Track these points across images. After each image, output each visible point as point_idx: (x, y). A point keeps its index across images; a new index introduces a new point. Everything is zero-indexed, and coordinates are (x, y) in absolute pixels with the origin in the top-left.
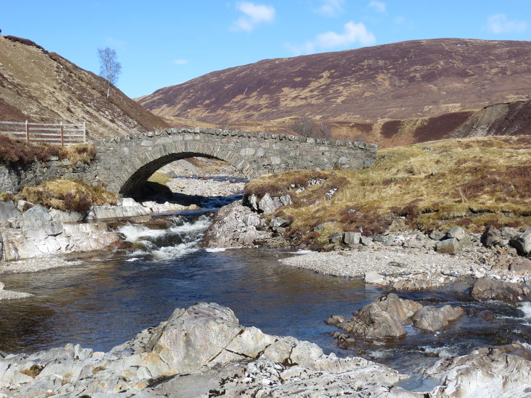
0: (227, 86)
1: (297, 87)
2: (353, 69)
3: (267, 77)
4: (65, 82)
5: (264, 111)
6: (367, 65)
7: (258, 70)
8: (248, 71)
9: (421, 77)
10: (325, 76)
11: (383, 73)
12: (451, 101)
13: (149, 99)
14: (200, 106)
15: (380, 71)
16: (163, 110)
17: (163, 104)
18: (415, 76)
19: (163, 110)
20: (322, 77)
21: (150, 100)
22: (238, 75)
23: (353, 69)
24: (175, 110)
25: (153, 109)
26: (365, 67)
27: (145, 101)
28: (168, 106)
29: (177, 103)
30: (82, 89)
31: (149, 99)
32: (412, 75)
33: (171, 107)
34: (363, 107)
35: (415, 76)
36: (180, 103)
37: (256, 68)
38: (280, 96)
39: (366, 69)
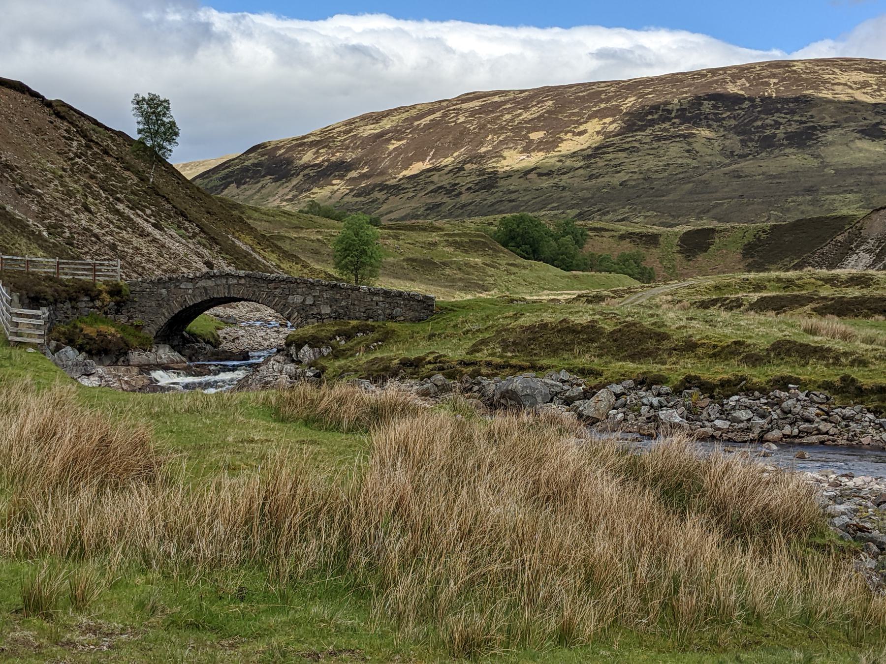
0: (393, 144)
1: (534, 150)
2: (650, 117)
3: (474, 129)
4: (80, 158)
5: (465, 198)
6: (678, 110)
7: (458, 114)
8: (438, 114)
9: (787, 138)
10: (590, 131)
11: (709, 126)
12: (842, 189)
13: (237, 165)
14: (338, 181)
15: (704, 122)
16: (263, 187)
17: (264, 176)
18: (775, 135)
19: (263, 187)
20: (584, 132)
21: (239, 167)
22: (416, 123)
23: (650, 117)
24: (287, 190)
25: (244, 184)
26: (673, 115)
27: (228, 167)
28: (275, 180)
29: (292, 175)
30: (107, 168)
31: (237, 165)
32: (768, 132)
33: (278, 183)
34: (663, 196)
35: (775, 135)
36: (298, 175)
37: (454, 109)
38: (497, 167)
39: (676, 117)
